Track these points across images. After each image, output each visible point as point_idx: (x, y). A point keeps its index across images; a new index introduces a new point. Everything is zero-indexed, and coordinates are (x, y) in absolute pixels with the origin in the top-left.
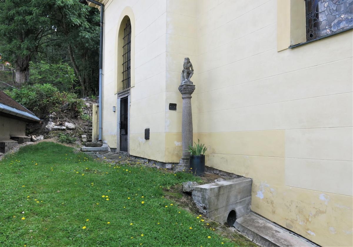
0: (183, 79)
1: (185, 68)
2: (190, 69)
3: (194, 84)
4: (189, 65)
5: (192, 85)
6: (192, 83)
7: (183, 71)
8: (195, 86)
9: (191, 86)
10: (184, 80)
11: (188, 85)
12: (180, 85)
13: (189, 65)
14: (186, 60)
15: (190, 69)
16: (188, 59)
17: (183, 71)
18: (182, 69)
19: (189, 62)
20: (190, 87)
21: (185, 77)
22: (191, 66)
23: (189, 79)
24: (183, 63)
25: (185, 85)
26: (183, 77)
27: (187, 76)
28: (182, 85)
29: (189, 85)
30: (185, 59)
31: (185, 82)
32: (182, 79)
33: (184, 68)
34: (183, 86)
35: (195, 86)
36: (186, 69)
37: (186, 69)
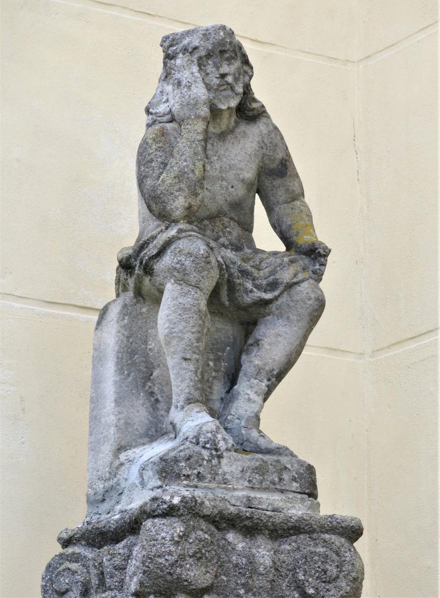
0: (140, 414)
1: (178, 204)
2: (264, 237)
3: (332, 504)
4: (241, 155)
5: (297, 510)
6: (311, 492)
7: (137, 271)
8: (353, 533)
9: (282, 531)
10: (157, 430)
11: (224, 522)
12: (77, 519)
13: (241, 155)
14: (188, 71)
15: (264, 237)
16: (223, 53)
17: (126, 265)
18: (128, 225)
19: (248, 111)
20: (263, 552)
21: (179, 377)
22: (275, 175)
23: (242, 407)
24: (137, 129)
25: (170, 512)
26: (140, 368)
27: (214, 349)
28: (113, 515)
29: (250, 526)
30: (172, 49)
31: (167, 469)
32: (109, 405)
33: (155, 205)
34: (132, 526)
35: (353, 533)
36: (190, 215)
37: (190, 215)
